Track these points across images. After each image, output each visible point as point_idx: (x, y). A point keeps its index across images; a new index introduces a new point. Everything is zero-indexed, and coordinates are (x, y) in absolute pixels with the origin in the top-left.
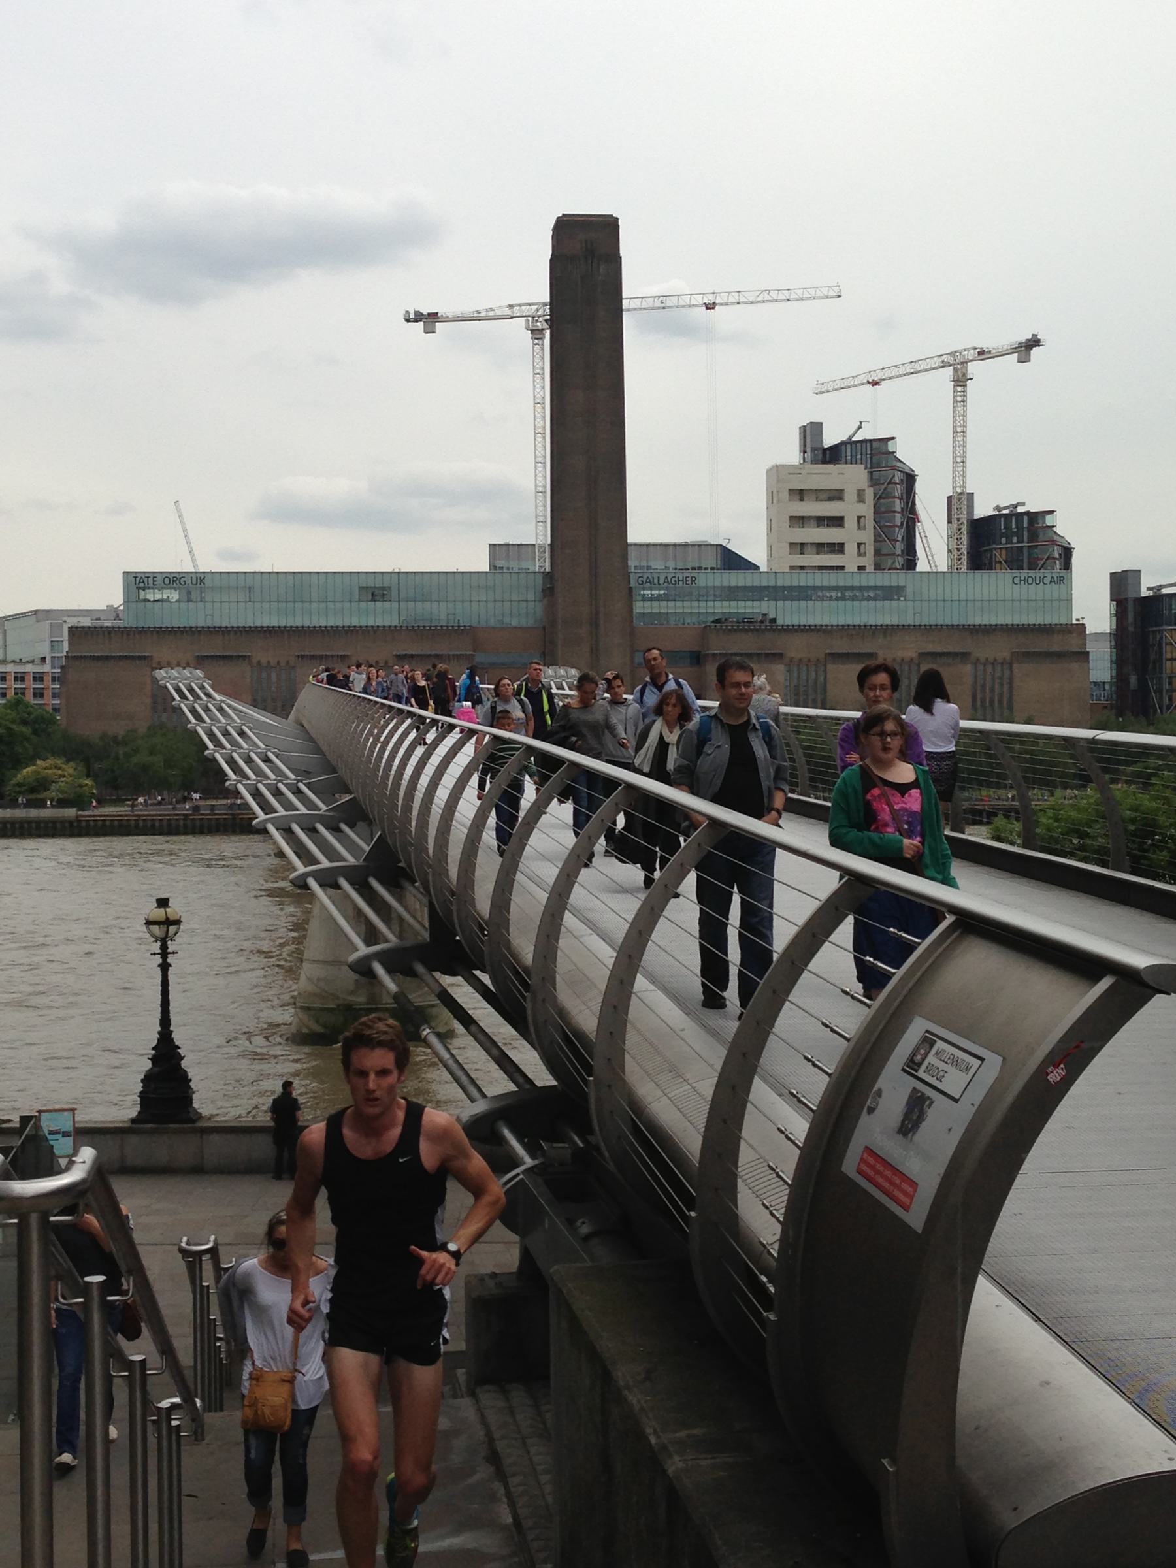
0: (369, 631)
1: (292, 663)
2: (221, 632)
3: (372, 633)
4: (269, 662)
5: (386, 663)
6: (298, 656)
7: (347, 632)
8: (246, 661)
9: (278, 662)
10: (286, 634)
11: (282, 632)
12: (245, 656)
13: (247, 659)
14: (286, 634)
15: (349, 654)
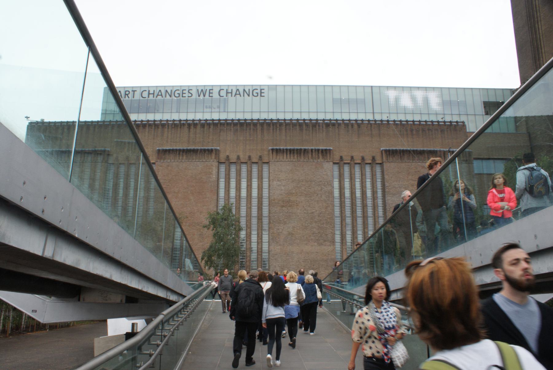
0: (352, 125)
1: (265, 159)
2: (186, 126)
3: (356, 126)
4: (238, 158)
5: (373, 159)
6: (273, 150)
7: (327, 125)
8: (213, 155)
9: (250, 157)
10: (259, 127)
11: (255, 125)
12: (212, 150)
13: (213, 156)
14: (259, 127)
15: (331, 148)
